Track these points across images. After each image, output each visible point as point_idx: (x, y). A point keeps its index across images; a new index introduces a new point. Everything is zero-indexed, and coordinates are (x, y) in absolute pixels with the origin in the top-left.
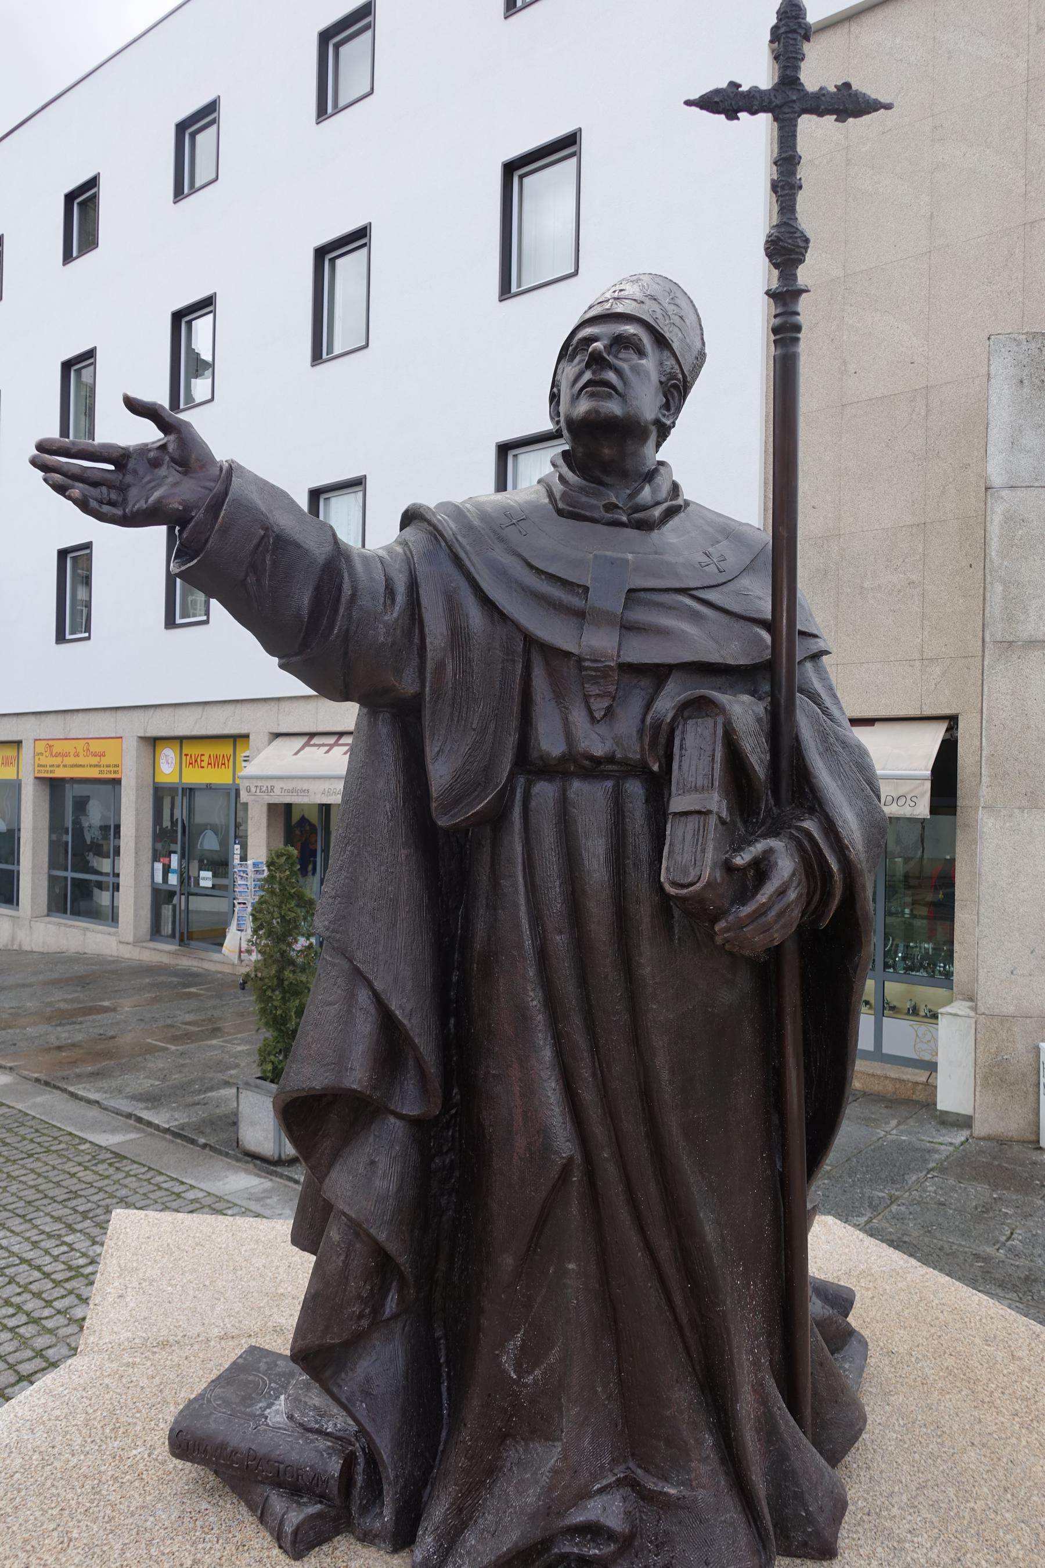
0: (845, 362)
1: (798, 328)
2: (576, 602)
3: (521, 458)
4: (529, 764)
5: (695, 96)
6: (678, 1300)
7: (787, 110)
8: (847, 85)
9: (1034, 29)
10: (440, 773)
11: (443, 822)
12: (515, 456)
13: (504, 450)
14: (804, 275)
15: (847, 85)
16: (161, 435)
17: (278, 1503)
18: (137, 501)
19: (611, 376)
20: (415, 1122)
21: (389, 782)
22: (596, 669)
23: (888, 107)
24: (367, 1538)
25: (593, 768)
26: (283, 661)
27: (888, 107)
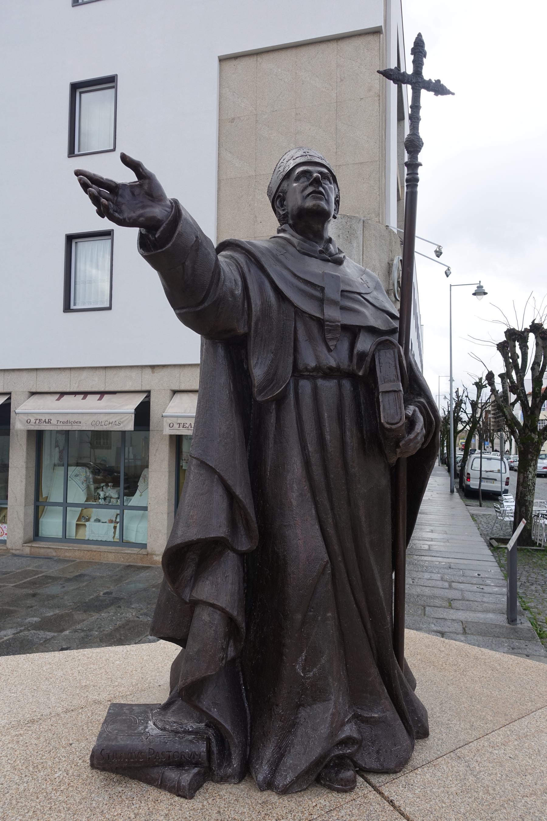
0: (256, 217)
1: (417, 180)
2: (318, 294)
3: (79, 244)
4: (298, 372)
5: (381, 70)
6: (369, 625)
7: (417, 85)
8: (439, 81)
9: (339, 80)
10: (258, 373)
11: (259, 399)
12: (76, 243)
13: (70, 239)
14: (421, 157)
15: (439, 81)
16: (136, 179)
17: (172, 774)
18: (127, 214)
19: (321, 189)
20: (242, 555)
21: (223, 379)
22: (331, 326)
23: (453, 94)
24: (223, 780)
25: (330, 373)
26: (178, 312)
27: (453, 94)
